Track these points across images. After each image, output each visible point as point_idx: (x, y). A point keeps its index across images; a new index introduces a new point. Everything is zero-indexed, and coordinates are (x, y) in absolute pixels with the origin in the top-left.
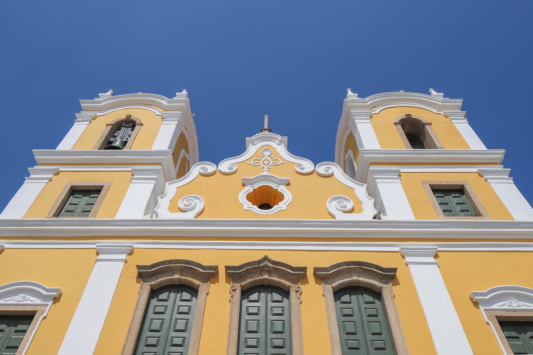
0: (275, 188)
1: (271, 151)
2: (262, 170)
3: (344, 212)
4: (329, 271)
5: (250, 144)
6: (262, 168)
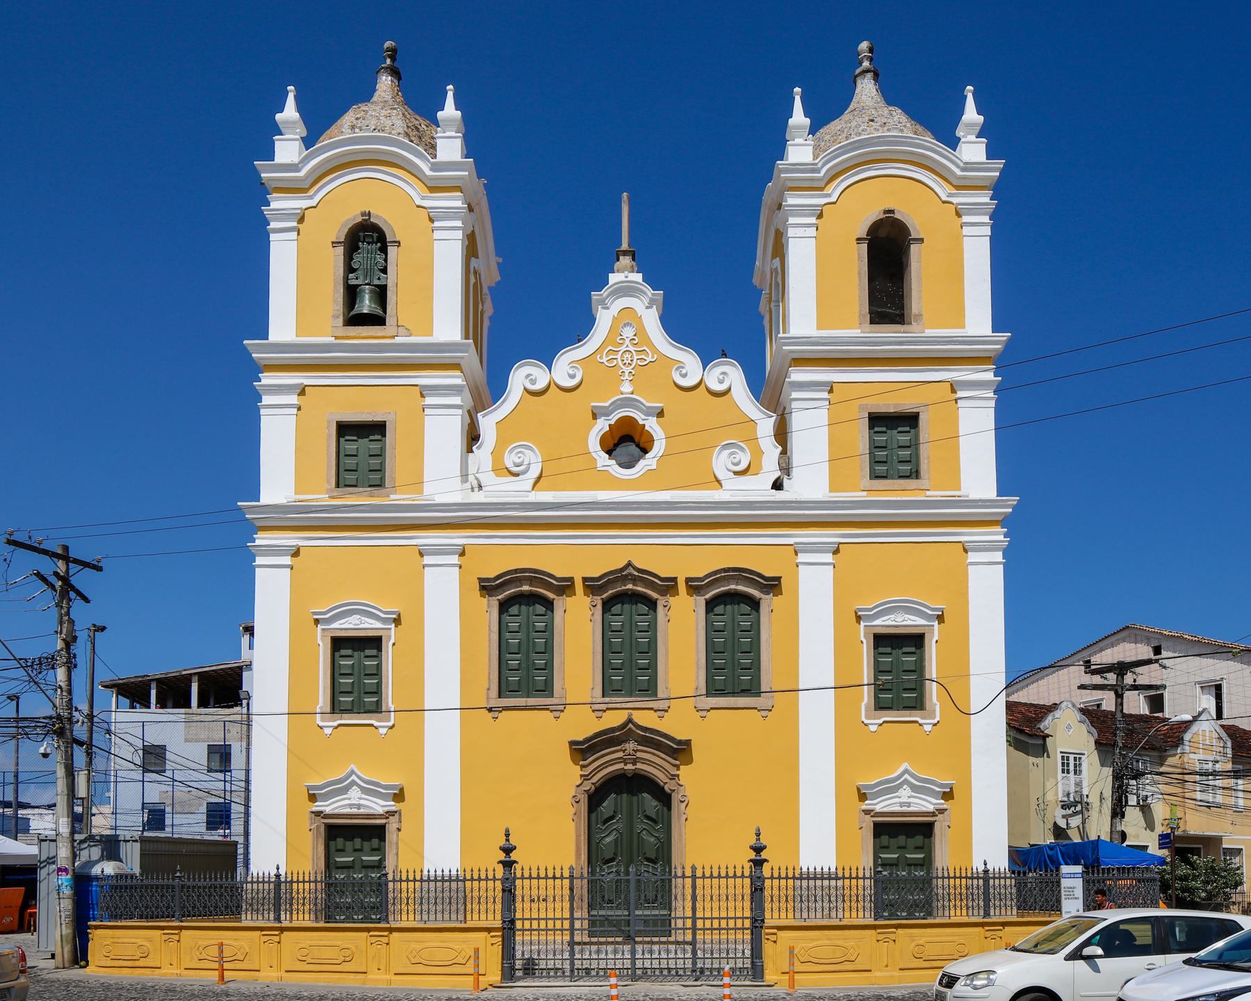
0: (641, 422)
1: (634, 329)
2: (622, 378)
3: (736, 473)
4: (703, 581)
5: (600, 307)
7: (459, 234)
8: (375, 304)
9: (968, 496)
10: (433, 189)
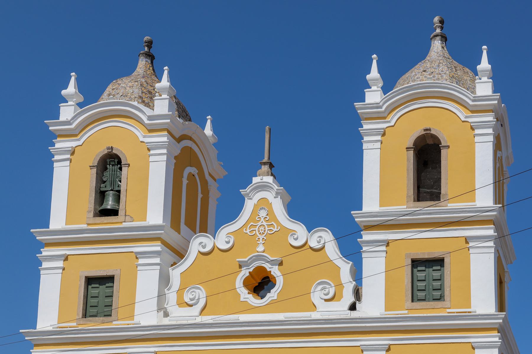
0: (268, 270)
1: (266, 210)
2: (258, 242)
3: (326, 300)
6: (258, 239)
7: (165, 158)
8: (114, 202)
9: (475, 312)
10: (150, 131)
